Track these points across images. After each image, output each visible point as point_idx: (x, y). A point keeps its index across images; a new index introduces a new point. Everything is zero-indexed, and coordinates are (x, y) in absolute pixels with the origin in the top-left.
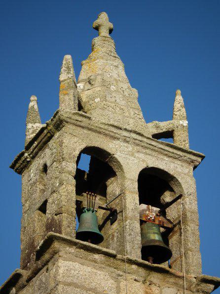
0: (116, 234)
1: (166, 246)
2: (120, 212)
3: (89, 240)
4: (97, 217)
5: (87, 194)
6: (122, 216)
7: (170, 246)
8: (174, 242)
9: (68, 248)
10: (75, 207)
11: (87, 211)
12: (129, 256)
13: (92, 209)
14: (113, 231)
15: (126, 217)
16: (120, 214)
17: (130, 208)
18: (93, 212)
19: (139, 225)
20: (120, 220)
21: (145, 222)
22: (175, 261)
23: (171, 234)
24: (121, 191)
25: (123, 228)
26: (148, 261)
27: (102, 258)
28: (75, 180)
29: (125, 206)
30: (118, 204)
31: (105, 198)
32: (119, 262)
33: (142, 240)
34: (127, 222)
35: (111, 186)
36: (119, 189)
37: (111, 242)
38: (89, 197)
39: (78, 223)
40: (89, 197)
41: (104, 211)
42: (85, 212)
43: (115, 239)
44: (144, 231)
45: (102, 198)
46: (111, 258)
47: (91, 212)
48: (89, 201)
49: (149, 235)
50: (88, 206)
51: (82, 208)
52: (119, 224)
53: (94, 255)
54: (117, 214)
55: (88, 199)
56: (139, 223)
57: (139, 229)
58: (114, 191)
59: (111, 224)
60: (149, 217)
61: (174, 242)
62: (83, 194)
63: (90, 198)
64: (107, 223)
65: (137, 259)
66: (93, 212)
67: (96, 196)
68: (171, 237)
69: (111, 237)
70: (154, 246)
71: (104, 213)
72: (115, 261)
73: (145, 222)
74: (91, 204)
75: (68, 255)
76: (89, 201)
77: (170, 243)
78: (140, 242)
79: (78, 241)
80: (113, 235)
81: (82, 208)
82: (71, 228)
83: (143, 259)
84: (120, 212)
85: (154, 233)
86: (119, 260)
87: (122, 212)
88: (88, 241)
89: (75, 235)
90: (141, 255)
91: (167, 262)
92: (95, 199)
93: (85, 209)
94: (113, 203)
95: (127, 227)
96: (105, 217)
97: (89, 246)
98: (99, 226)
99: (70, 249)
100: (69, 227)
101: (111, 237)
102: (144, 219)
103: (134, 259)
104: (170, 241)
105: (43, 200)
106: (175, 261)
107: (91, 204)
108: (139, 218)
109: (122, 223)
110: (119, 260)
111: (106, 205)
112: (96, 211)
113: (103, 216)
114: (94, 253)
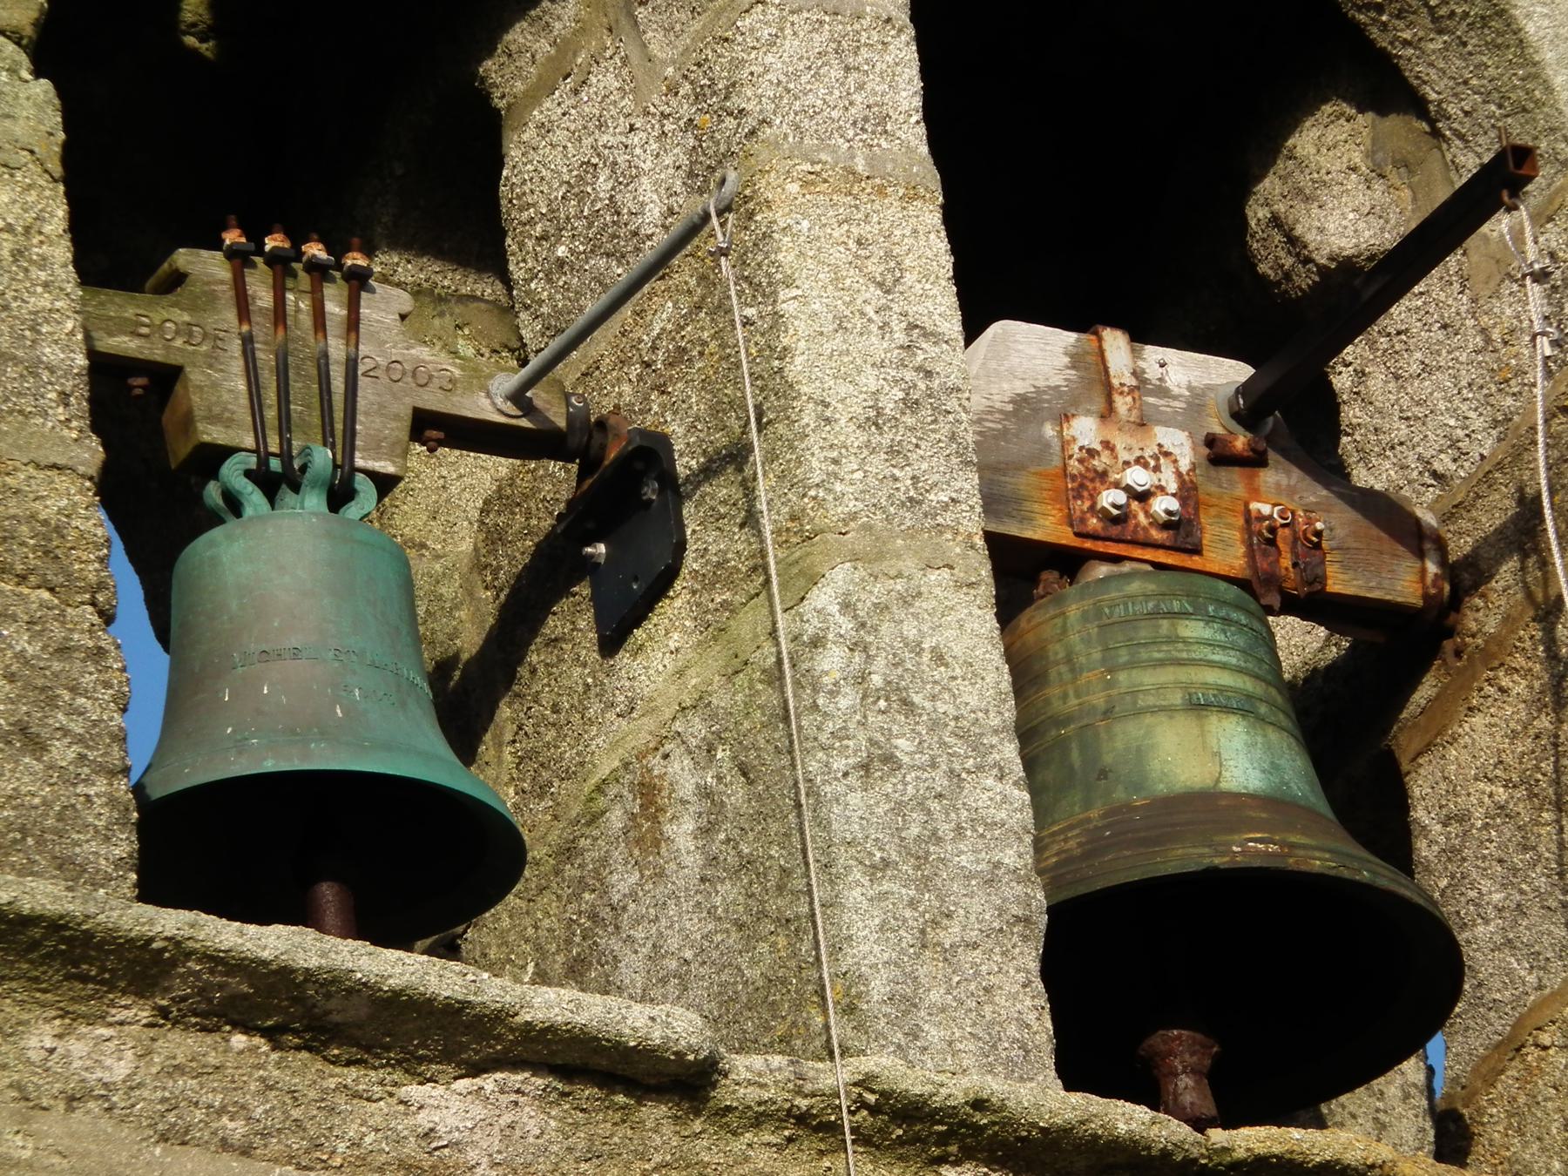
0: (682, 775)
1: (1369, 870)
2: (708, 472)
3: (328, 893)
4: (400, 558)
5: (239, 259)
6: (751, 520)
7: (1424, 850)
8: (1479, 798)
9: (40, 1037)
10: (91, 454)
11: (254, 499)
12: (882, 1063)
13: (322, 458)
14: (641, 731)
15: (800, 532)
16: (723, 489)
17: (849, 403)
18: (339, 496)
19: (986, 621)
20: (719, 574)
21: (1068, 562)
22: (1512, 1046)
23: (1425, 691)
24: (700, 175)
25: (775, 677)
26: (1150, 1094)
27: (530, 1119)
28: (43, 88)
29: (774, 385)
30: (680, 356)
31: (489, 288)
32: (758, 1147)
33: (1042, 808)
34: (823, 598)
35: (548, 109)
36: (677, 155)
37: (623, 881)
38: (261, 294)
39: (152, 665)
40: (261, 294)
41: (496, 467)
42: (234, 504)
43: (682, 832)
44: (1060, 697)
45: (449, 279)
46: (654, 1113)
47: (314, 501)
48: (265, 358)
49: (1126, 734)
50: (259, 429)
51: (180, 451)
52: (713, 630)
53: (414, 1091)
54: (673, 490)
55: (262, 328)
56: (987, 590)
57: (998, 676)
58: (603, 183)
59: (612, 642)
60: (1110, 498)
61: (1479, 798)
62: (183, 258)
63: (279, 314)
64: (554, 625)
65: (995, 1086)
66: (339, 496)
67: (359, 281)
68: (1436, 734)
69: (616, 819)
70: (1212, 876)
71: (501, 499)
72: (708, 1148)
73: (1068, 562)
74: (303, 390)
75: (53, 1126)
76: (265, 358)
77: (1419, 814)
78: (1016, 855)
79: (170, 922)
80: (648, 792)
81: (180, 451)
82: (63, 753)
83: (1074, 1074)
84: (708, 472)
85: (1198, 706)
86: (758, 1118)
87: (736, 456)
88: (299, 913)
89: (125, 845)
90: (1042, 1029)
91: (1411, 1069)
92: (353, 323)
93: (233, 472)
94: (600, 345)
95: (832, 662)
96: (516, 556)
97: (334, 984)
98: (440, 672)
99: (76, 1048)
100: (37, 746)
101: (616, 819)
102: (1047, 527)
103: (955, 1090)
104: (1424, 788)
105: (145, 1030)
106: (1512, 1046)
107: (303, 390)
108: (972, 523)
109: (748, 623)
110: (758, 1118)
111: (505, 382)
112: (385, 484)
113: (493, 537)
114: (412, 1066)
